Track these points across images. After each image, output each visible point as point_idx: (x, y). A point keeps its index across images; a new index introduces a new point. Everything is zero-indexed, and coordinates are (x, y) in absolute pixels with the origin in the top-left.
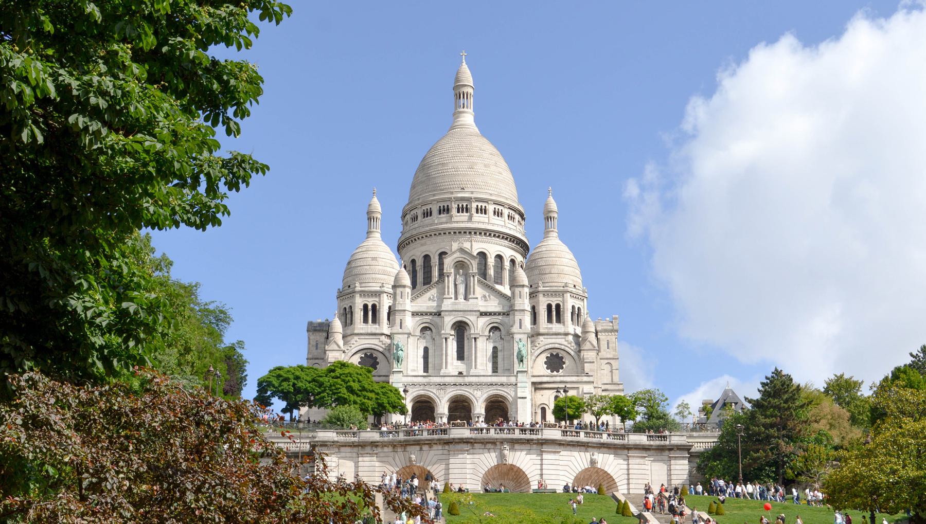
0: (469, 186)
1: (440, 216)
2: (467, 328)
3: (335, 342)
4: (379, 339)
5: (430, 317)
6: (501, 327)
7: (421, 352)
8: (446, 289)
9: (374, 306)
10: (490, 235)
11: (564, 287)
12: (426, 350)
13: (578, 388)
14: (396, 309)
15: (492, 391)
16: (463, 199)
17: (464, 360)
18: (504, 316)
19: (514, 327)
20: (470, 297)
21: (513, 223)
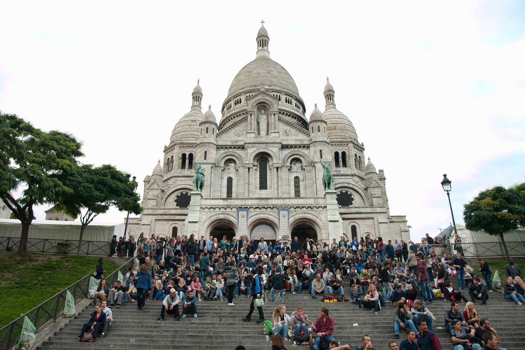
0: (267, 83)
2: (270, 159)
5: (235, 150)
6: (301, 158)
7: (225, 182)
9: (191, 156)
10: (283, 113)
11: (347, 139)
12: (230, 180)
13: (373, 218)
14: (202, 142)
15: (300, 214)
17: (266, 189)
18: (305, 149)
20: (272, 131)
21: (299, 110)
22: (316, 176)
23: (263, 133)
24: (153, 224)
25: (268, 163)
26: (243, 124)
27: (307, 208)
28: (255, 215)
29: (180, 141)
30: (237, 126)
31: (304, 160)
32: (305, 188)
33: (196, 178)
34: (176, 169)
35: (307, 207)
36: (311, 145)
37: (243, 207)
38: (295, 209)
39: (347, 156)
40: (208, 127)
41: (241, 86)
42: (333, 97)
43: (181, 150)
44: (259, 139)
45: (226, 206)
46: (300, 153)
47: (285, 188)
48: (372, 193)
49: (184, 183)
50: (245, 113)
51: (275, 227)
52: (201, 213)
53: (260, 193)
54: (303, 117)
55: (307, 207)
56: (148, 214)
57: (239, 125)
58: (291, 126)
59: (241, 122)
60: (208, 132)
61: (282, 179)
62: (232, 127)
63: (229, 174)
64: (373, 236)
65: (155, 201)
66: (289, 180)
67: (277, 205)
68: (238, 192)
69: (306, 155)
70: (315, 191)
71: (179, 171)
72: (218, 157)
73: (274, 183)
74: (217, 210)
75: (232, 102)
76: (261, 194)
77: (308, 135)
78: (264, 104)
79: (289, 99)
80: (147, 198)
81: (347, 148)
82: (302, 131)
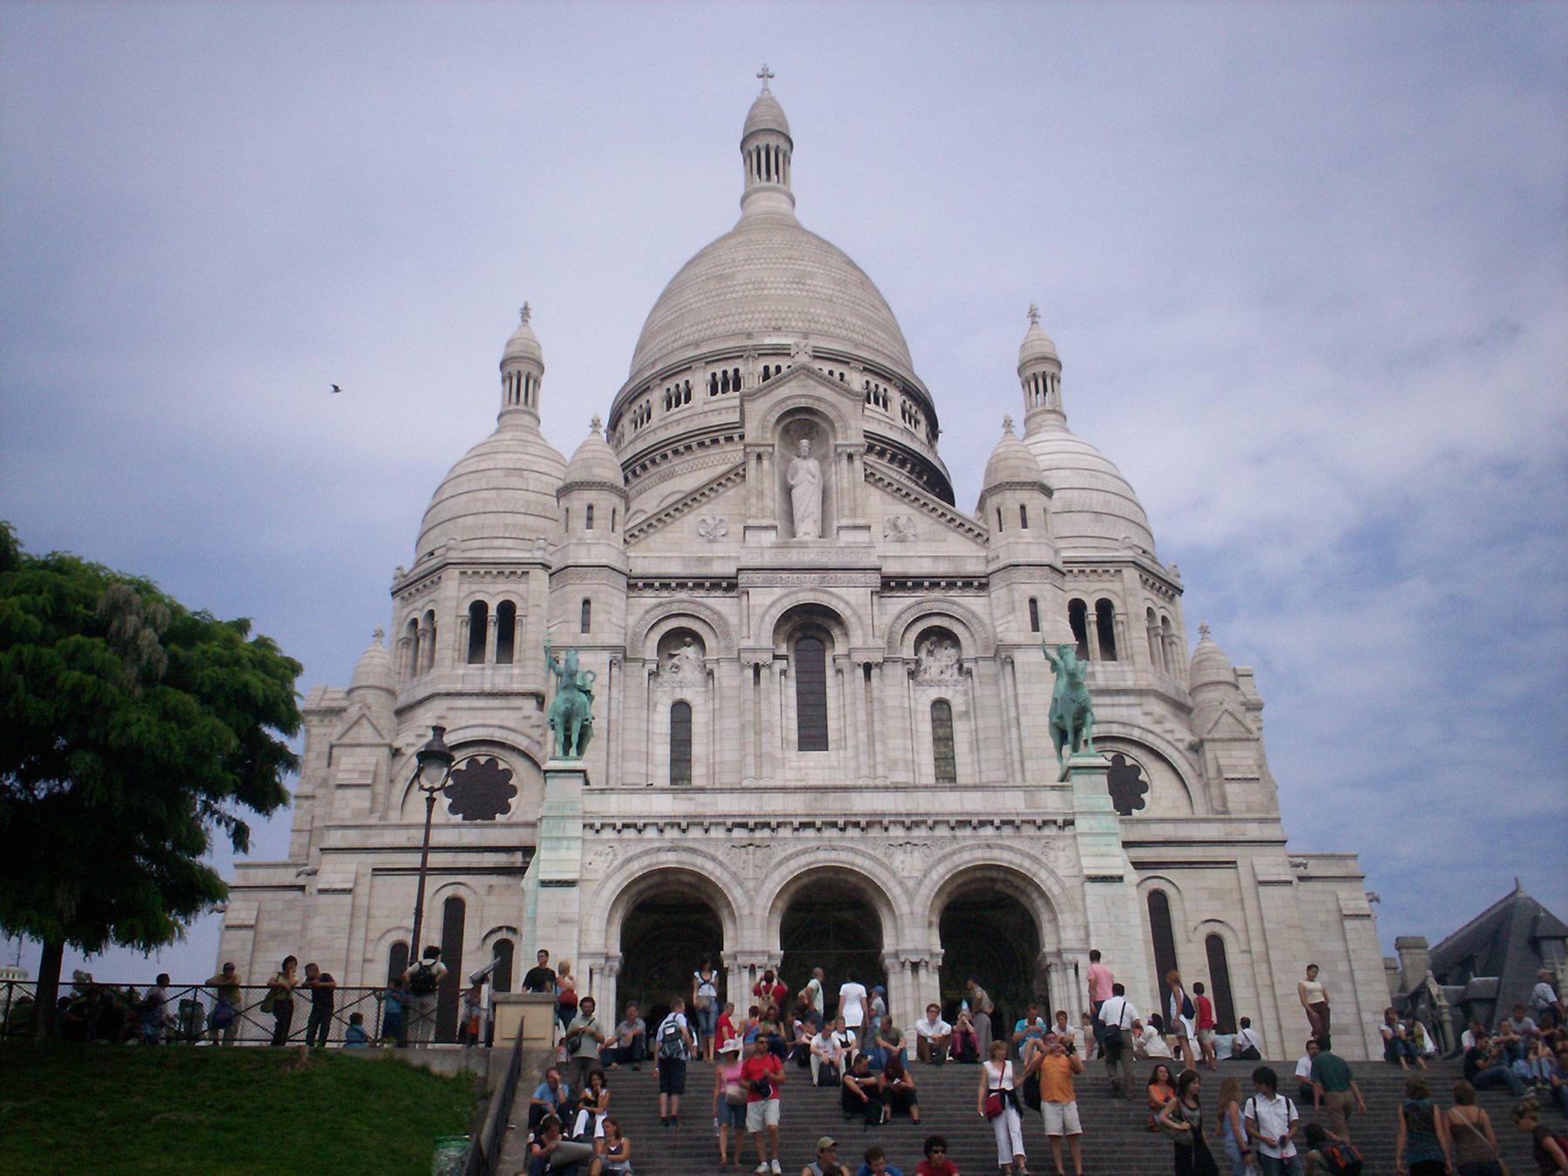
0: (793, 324)
1: (714, 398)
2: (836, 632)
3: (364, 715)
4: (519, 709)
6: (958, 629)
8: (753, 500)
9: (507, 610)
12: (681, 712)
13: (1231, 864)
14: (570, 562)
15: (971, 852)
16: (781, 351)
18: (971, 592)
19: (1014, 625)
20: (844, 522)
21: (913, 430)
22: (1021, 701)
23: (807, 528)
24: (362, 890)
25: (828, 645)
26: (730, 493)
27: (998, 828)
28: (797, 854)
29: (464, 551)
30: (704, 500)
31: (967, 635)
32: (976, 746)
33: (562, 708)
34: (448, 662)
35: (997, 822)
36: (993, 579)
37: (751, 822)
38: (953, 828)
39: (1119, 618)
40: (594, 503)
41: (690, 334)
42: (1055, 383)
43: (466, 589)
44: (794, 551)
45: (685, 817)
46: (952, 610)
47: (896, 745)
48: (1222, 762)
49: (480, 722)
50: (708, 442)
51: (877, 899)
52: (588, 846)
53: (802, 764)
54: (930, 457)
55: (997, 822)
56: (344, 846)
57: (713, 495)
58: (915, 504)
59: (720, 484)
60: (596, 523)
61: (883, 711)
62: (686, 504)
63: (678, 690)
64: (1236, 936)
65: (366, 792)
66: (911, 713)
67: (884, 815)
68: (717, 760)
69: (975, 615)
70: (1016, 757)
71: (461, 672)
72: (632, 620)
73: (855, 725)
74: (651, 833)
75: (656, 397)
76: (807, 767)
77: (981, 538)
78: (807, 417)
79: (877, 386)
80: (333, 782)
81: (1117, 586)
82: (958, 522)
